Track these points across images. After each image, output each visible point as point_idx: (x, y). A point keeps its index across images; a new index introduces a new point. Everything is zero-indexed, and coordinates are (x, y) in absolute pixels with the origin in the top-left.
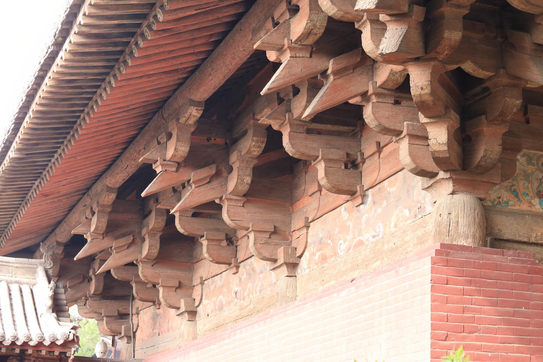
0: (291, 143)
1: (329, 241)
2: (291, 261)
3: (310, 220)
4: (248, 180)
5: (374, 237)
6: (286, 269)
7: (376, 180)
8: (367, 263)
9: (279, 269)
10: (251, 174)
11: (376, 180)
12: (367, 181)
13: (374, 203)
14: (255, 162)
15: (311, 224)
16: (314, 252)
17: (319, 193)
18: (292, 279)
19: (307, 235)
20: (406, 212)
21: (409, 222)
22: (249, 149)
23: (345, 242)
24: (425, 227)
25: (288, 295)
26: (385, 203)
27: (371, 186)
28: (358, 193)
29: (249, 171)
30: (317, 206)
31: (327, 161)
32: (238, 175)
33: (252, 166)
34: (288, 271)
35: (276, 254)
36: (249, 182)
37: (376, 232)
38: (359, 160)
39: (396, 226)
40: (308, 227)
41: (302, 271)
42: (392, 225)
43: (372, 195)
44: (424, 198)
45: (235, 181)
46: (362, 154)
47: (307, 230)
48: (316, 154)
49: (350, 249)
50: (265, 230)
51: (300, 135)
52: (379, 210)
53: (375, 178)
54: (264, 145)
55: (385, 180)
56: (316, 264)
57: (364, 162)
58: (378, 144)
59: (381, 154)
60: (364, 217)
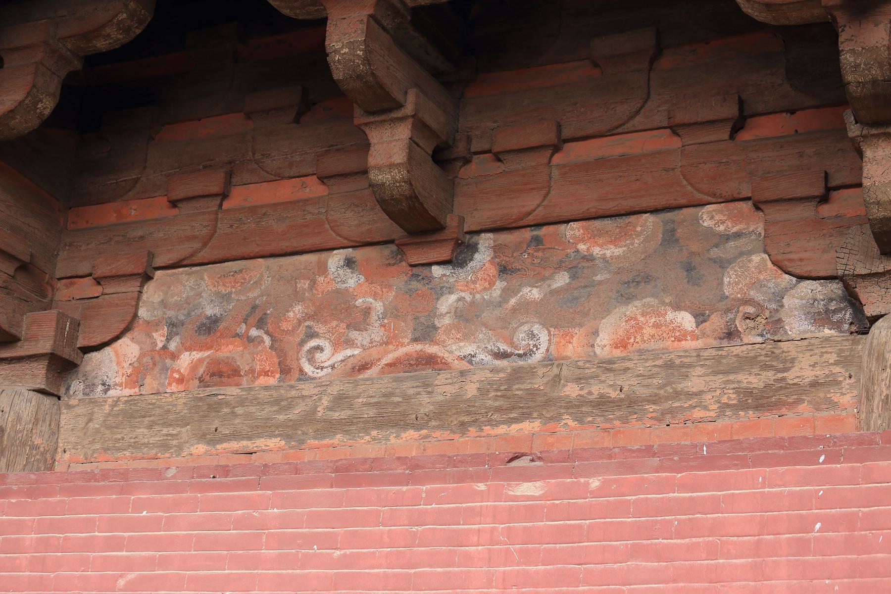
0: (367, 46)
1: (254, 332)
2: (67, 353)
3: (158, 262)
4: (47, 106)
5: (504, 355)
6: (44, 372)
7: (529, 213)
8: (466, 419)
9: (17, 366)
10: (58, 94)
11: (529, 213)
12: (471, 210)
13: (504, 270)
14: (78, 65)
15: (159, 274)
16: (173, 346)
17: (217, 201)
18: (47, 401)
19: (139, 299)
20: (686, 320)
21: (689, 344)
22: (104, 26)
23: (337, 345)
24: (786, 370)
25: (37, 441)
26: (562, 279)
27: (499, 224)
28: (449, 233)
29: (54, 87)
30: (205, 232)
31: (420, 126)
32: (34, 86)
33: (63, 74)
34: (47, 378)
35: (19, 325)
36: (47, 112)
37: (511, 343)
38: (460, 149)
39: (621, 344)
40: (147, 277)
41: (91, 387)
42: (604, 339)
43: (497, 249)
44: (779, 297)
45: (19, 96)
46: (469, 140)
47: (142, 286)
48: (400, 97)
49: (364, 367)
50: (14, 253)
51: (384, 36)
52: (534, 294)
53: (533, 207)
54: (138, 31)
55: (567, 222)
56: (180, 381)
57: (467, 161)
58: (559, 127)
59: (556, 156)
60: (453, 298)
